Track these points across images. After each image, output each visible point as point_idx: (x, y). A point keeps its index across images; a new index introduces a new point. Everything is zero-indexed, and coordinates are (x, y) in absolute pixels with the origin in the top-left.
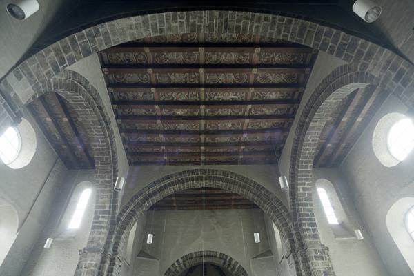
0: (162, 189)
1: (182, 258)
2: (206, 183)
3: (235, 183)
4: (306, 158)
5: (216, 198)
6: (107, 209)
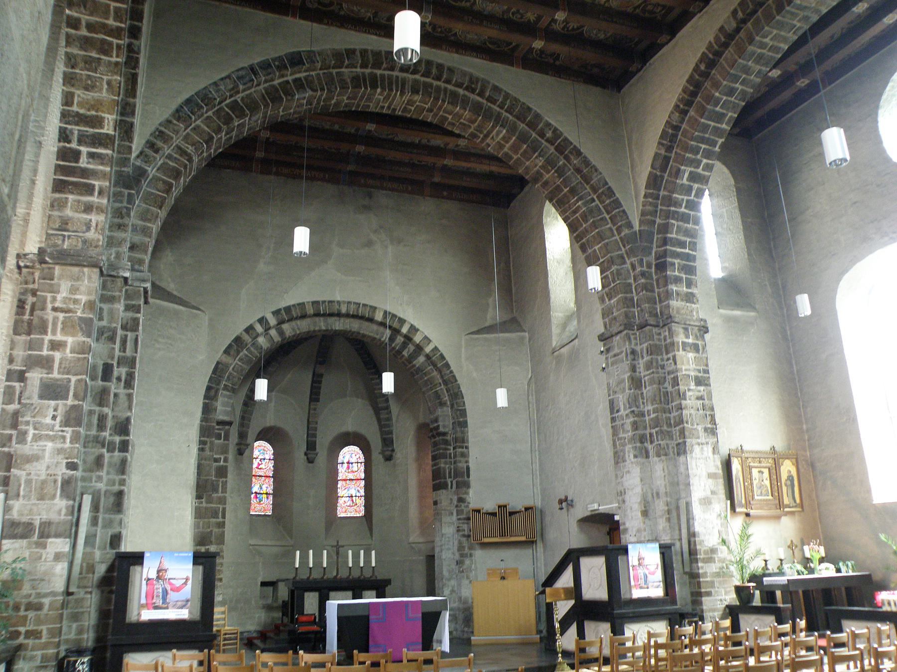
0: (273, 96)
1: (276, 313)
2: (410, 102)
3: (498, 120)
4: (731, 92)
5: (392, 155)
6: (108, 129)
